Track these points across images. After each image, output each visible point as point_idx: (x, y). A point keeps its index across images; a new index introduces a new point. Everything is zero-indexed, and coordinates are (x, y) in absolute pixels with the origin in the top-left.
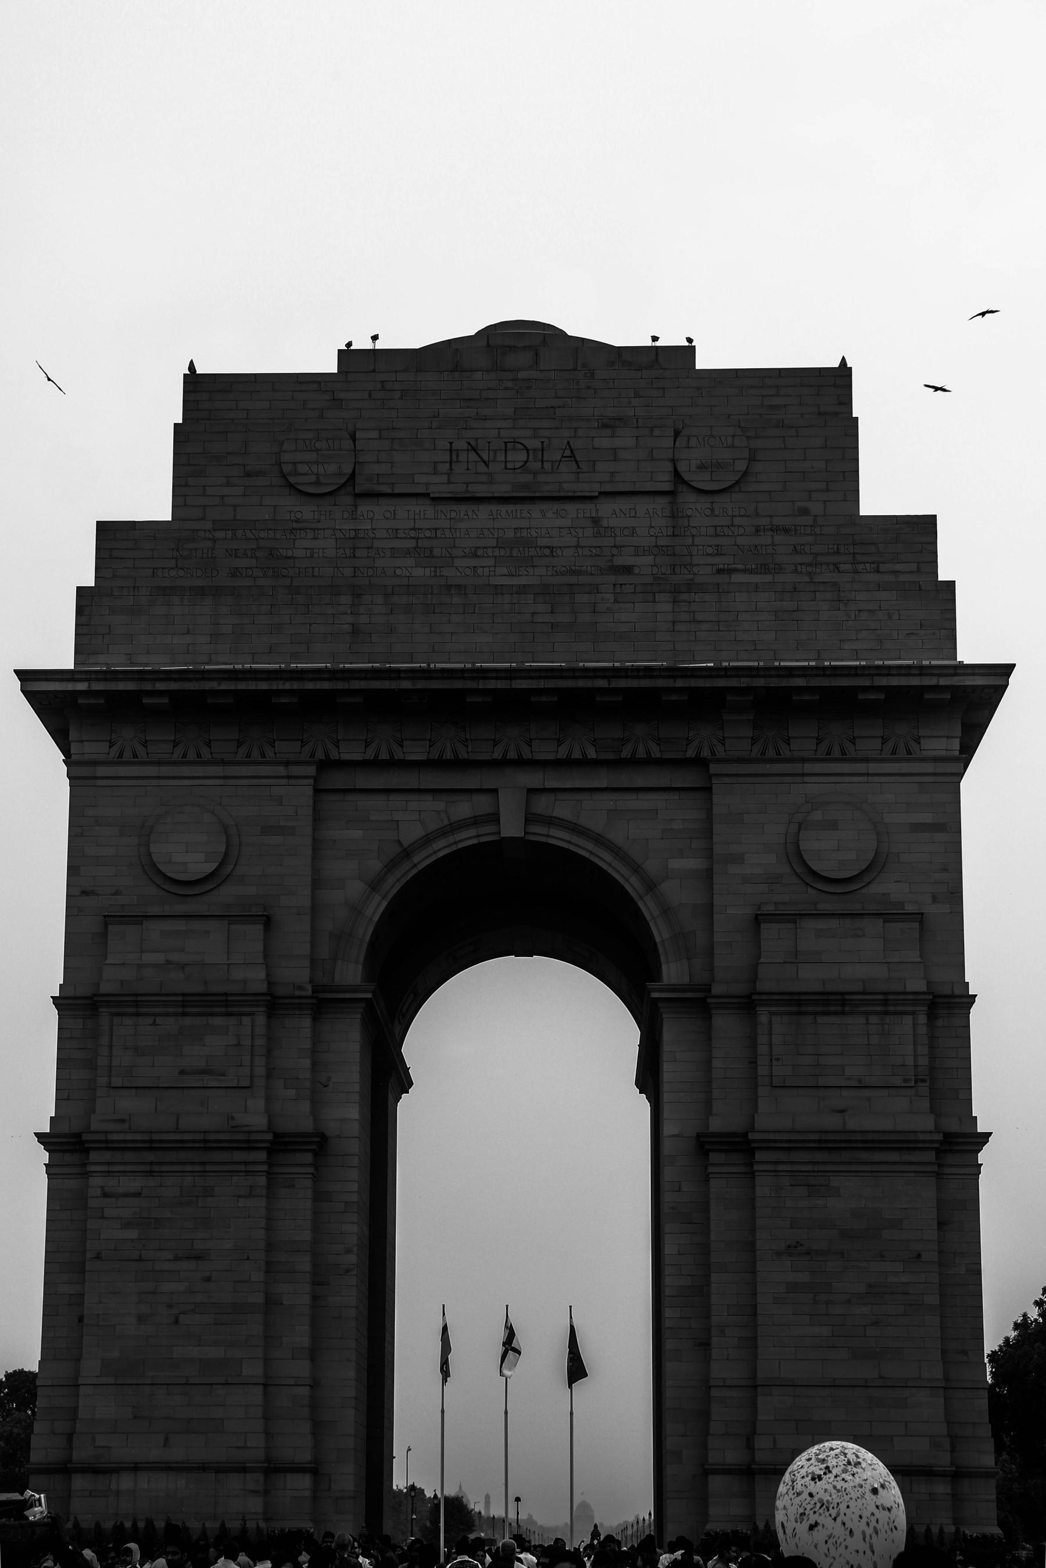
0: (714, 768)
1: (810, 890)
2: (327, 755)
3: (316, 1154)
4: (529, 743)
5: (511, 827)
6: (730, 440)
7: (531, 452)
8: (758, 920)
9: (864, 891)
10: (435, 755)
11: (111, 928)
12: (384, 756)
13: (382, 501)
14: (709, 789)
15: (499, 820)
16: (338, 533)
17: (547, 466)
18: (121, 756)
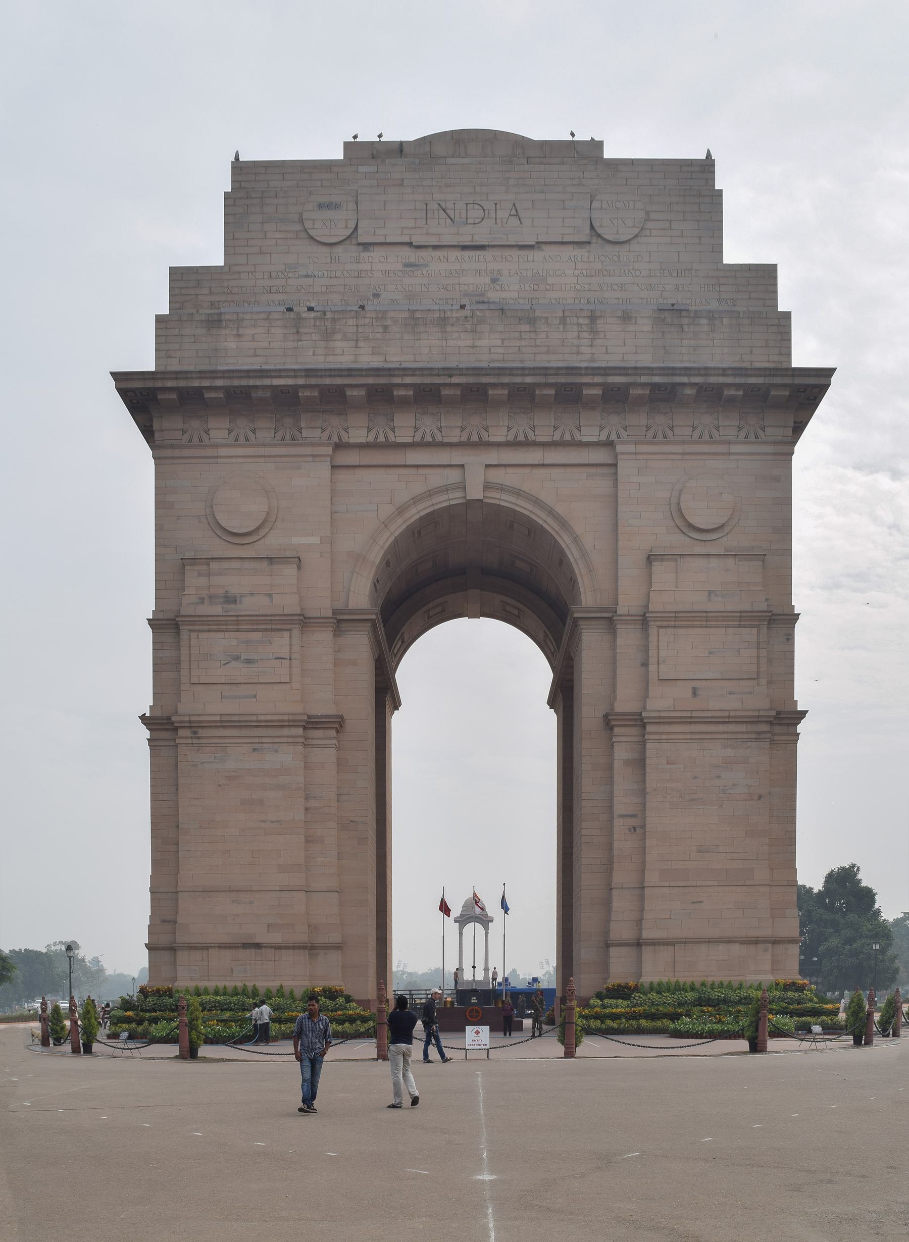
0: (619, 448)
1: (687, 539)
2: (340, 438)
3: (338, 732)
4: (486, 429)
5: (475, 492)
6: (631, 204)
7: (487, 212)
8: (650, 559)
9: (725, 539)
10: (418, 438)
11: (186, 567)
12: (381, 439)
13: (377, 248)
14: (615, 465)
15: (464, 488)
16: (345, 272)
17: (499, 221)
18: (190, 441)
